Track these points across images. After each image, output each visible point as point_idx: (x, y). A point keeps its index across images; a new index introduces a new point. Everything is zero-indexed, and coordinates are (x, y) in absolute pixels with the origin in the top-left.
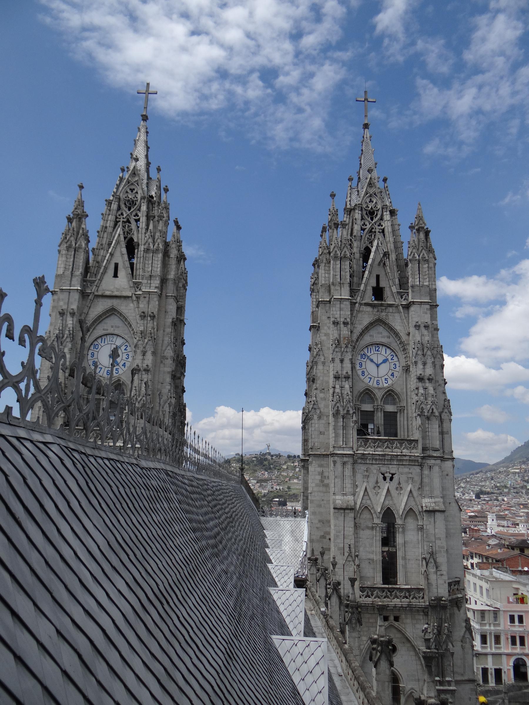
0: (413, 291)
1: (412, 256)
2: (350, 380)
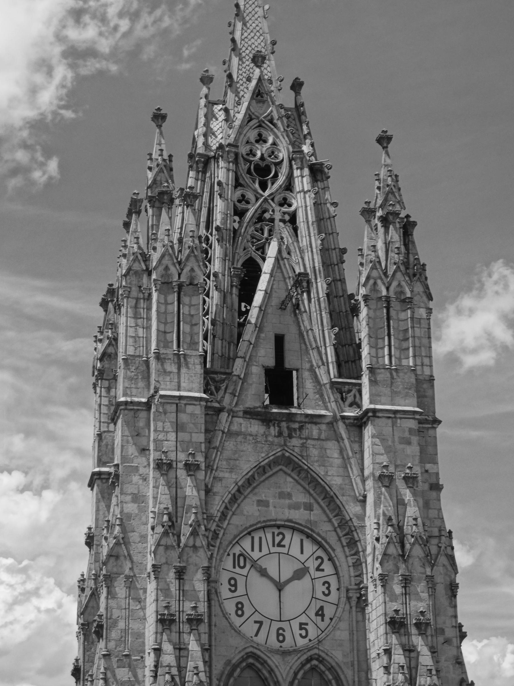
0: (373, 382)
1: (369, 287)
2: (203, 628)
